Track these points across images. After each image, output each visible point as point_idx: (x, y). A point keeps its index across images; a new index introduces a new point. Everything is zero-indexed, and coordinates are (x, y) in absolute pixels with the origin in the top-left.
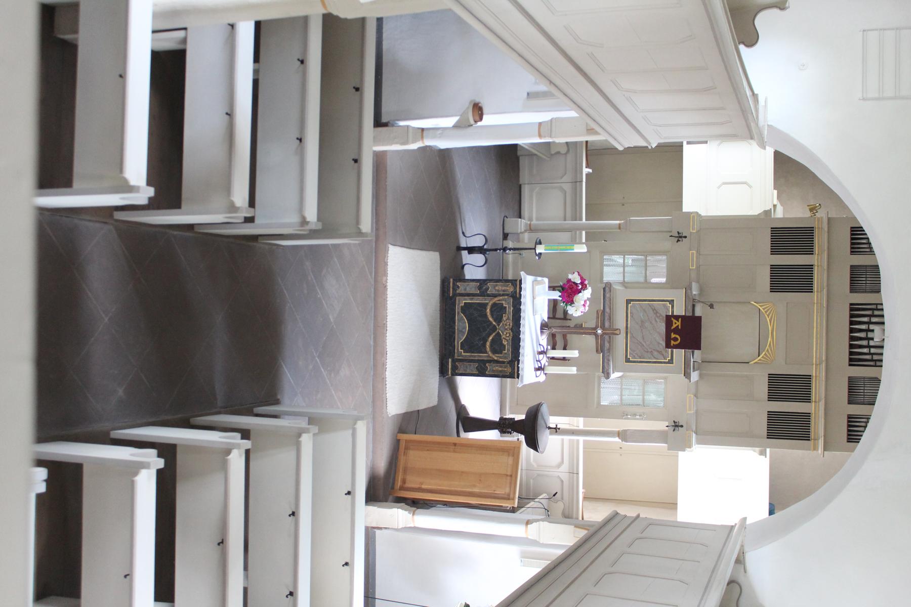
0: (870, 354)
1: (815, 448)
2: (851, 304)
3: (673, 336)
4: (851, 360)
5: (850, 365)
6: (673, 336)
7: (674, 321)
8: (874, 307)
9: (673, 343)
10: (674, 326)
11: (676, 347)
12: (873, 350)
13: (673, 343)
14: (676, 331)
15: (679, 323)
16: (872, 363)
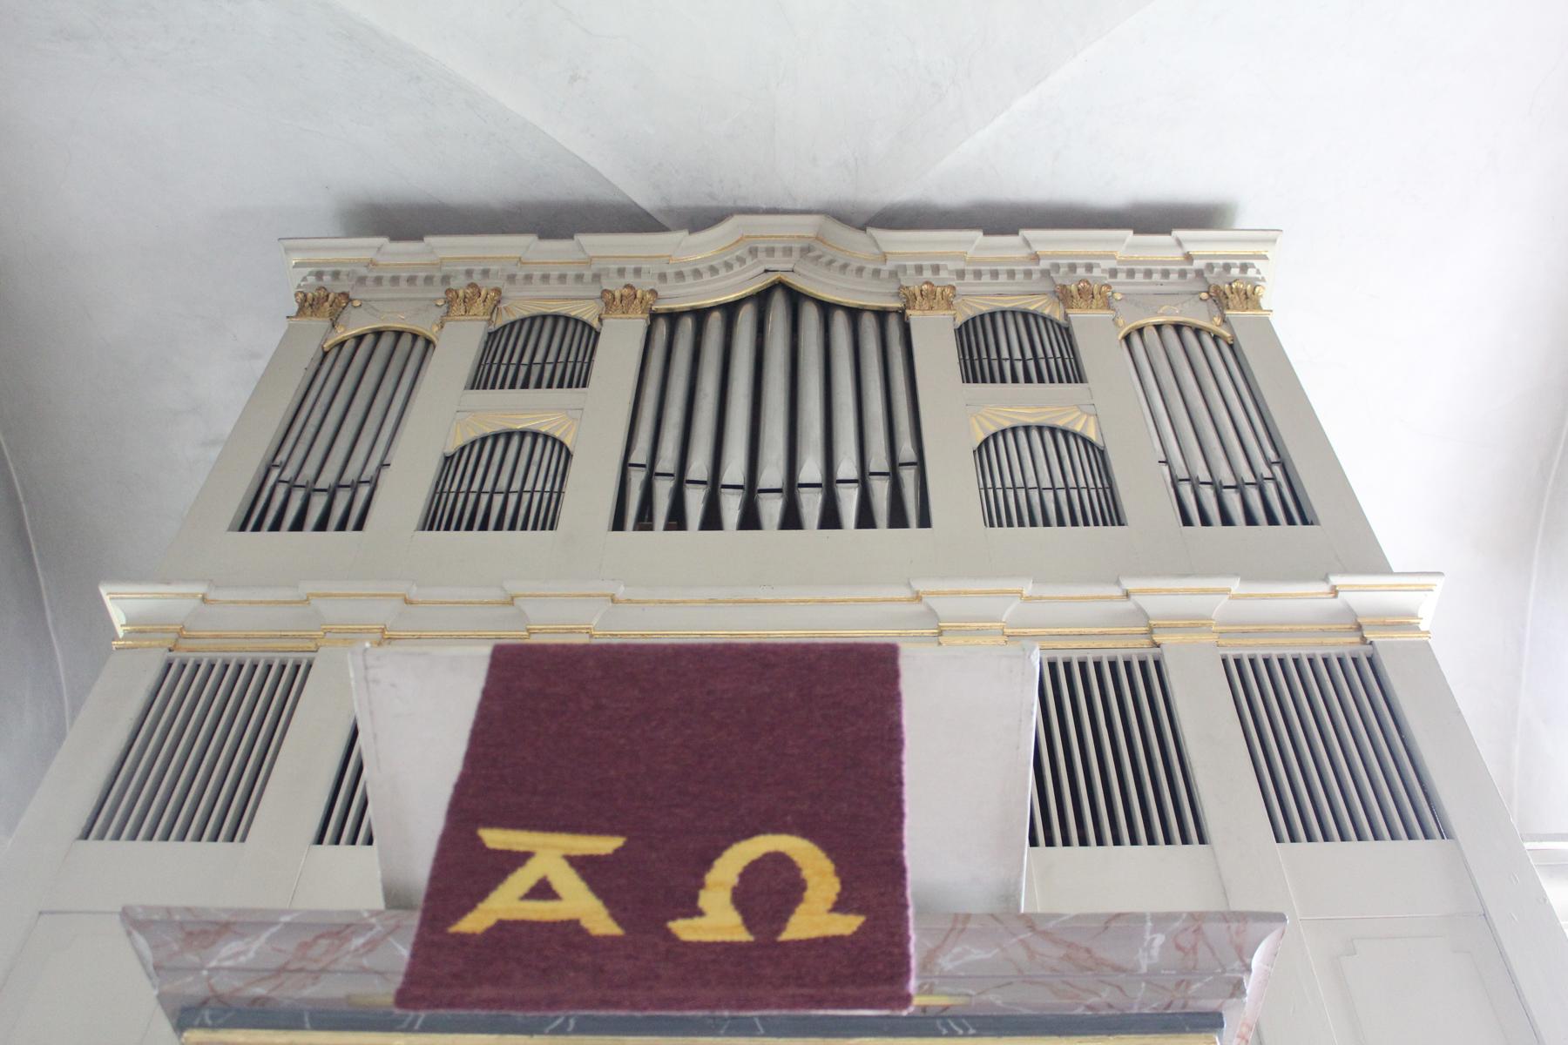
0: (863, 481)
1: (1403, 622)
2: (618, 524)
3: (716, 919)
4: (898, 519)
5: (925, 521)
6: (716, 919)
7: (507, 902)
8: (637, 478)
9: (817, 917)
10: (581, 905)
11: (874, 869)
12: (847, 467)
13: (817, 917)
14: (645, 889)
15: (549, 853)
16: (908, 476)
